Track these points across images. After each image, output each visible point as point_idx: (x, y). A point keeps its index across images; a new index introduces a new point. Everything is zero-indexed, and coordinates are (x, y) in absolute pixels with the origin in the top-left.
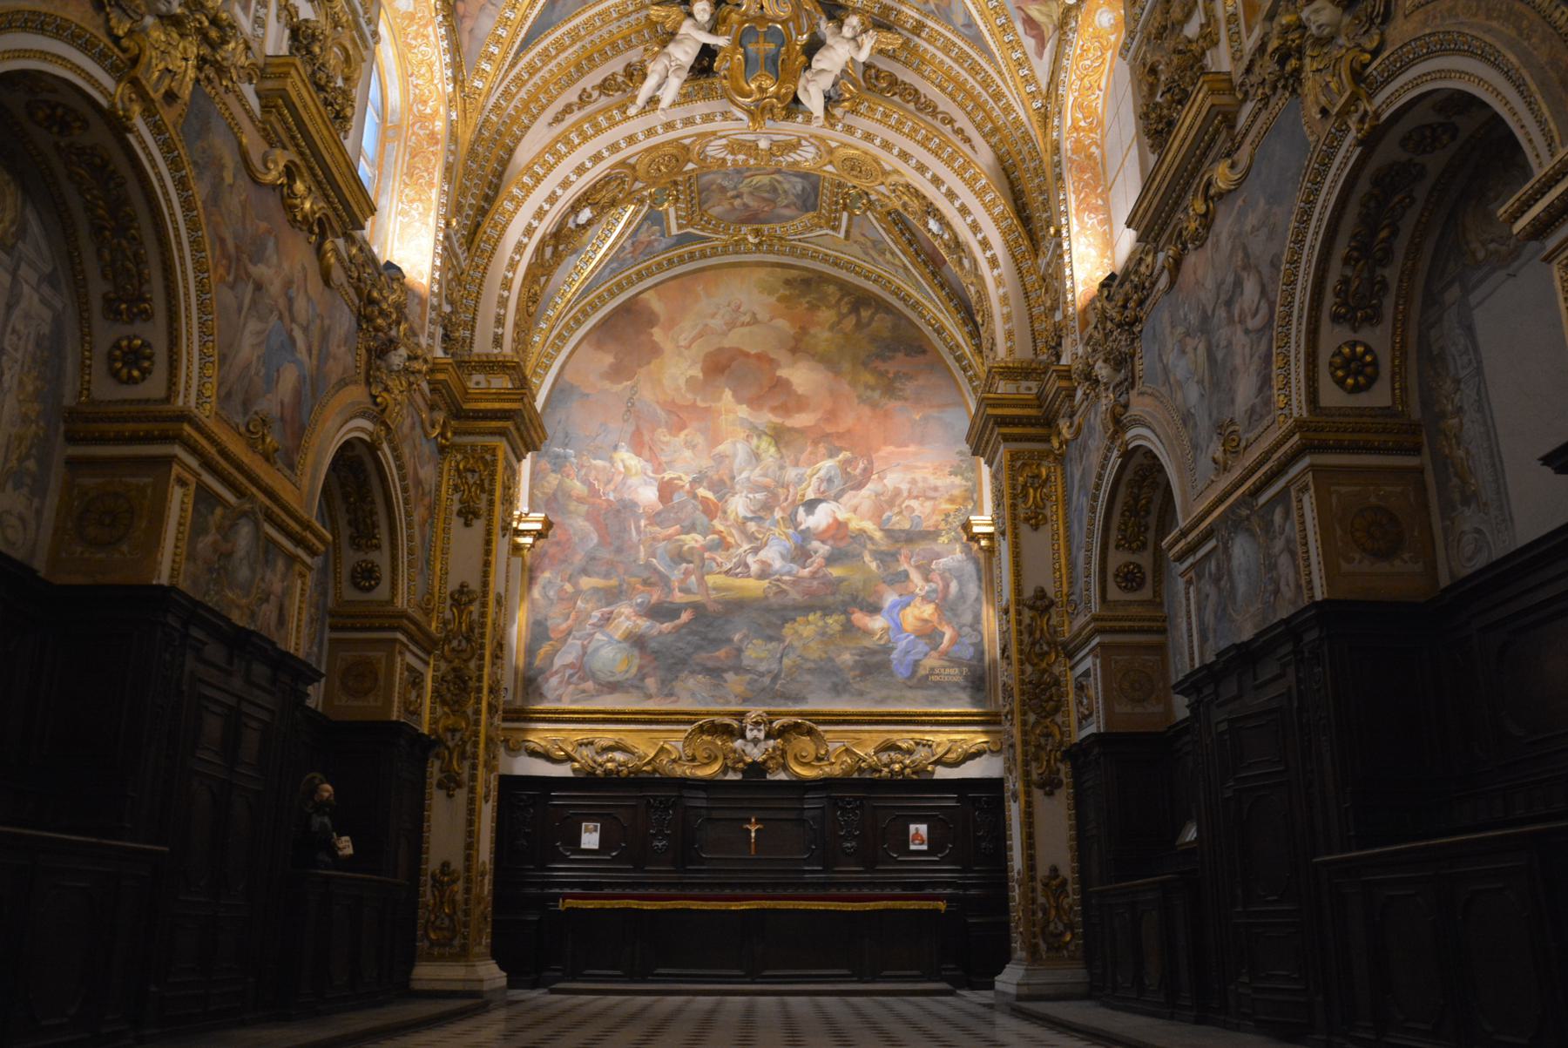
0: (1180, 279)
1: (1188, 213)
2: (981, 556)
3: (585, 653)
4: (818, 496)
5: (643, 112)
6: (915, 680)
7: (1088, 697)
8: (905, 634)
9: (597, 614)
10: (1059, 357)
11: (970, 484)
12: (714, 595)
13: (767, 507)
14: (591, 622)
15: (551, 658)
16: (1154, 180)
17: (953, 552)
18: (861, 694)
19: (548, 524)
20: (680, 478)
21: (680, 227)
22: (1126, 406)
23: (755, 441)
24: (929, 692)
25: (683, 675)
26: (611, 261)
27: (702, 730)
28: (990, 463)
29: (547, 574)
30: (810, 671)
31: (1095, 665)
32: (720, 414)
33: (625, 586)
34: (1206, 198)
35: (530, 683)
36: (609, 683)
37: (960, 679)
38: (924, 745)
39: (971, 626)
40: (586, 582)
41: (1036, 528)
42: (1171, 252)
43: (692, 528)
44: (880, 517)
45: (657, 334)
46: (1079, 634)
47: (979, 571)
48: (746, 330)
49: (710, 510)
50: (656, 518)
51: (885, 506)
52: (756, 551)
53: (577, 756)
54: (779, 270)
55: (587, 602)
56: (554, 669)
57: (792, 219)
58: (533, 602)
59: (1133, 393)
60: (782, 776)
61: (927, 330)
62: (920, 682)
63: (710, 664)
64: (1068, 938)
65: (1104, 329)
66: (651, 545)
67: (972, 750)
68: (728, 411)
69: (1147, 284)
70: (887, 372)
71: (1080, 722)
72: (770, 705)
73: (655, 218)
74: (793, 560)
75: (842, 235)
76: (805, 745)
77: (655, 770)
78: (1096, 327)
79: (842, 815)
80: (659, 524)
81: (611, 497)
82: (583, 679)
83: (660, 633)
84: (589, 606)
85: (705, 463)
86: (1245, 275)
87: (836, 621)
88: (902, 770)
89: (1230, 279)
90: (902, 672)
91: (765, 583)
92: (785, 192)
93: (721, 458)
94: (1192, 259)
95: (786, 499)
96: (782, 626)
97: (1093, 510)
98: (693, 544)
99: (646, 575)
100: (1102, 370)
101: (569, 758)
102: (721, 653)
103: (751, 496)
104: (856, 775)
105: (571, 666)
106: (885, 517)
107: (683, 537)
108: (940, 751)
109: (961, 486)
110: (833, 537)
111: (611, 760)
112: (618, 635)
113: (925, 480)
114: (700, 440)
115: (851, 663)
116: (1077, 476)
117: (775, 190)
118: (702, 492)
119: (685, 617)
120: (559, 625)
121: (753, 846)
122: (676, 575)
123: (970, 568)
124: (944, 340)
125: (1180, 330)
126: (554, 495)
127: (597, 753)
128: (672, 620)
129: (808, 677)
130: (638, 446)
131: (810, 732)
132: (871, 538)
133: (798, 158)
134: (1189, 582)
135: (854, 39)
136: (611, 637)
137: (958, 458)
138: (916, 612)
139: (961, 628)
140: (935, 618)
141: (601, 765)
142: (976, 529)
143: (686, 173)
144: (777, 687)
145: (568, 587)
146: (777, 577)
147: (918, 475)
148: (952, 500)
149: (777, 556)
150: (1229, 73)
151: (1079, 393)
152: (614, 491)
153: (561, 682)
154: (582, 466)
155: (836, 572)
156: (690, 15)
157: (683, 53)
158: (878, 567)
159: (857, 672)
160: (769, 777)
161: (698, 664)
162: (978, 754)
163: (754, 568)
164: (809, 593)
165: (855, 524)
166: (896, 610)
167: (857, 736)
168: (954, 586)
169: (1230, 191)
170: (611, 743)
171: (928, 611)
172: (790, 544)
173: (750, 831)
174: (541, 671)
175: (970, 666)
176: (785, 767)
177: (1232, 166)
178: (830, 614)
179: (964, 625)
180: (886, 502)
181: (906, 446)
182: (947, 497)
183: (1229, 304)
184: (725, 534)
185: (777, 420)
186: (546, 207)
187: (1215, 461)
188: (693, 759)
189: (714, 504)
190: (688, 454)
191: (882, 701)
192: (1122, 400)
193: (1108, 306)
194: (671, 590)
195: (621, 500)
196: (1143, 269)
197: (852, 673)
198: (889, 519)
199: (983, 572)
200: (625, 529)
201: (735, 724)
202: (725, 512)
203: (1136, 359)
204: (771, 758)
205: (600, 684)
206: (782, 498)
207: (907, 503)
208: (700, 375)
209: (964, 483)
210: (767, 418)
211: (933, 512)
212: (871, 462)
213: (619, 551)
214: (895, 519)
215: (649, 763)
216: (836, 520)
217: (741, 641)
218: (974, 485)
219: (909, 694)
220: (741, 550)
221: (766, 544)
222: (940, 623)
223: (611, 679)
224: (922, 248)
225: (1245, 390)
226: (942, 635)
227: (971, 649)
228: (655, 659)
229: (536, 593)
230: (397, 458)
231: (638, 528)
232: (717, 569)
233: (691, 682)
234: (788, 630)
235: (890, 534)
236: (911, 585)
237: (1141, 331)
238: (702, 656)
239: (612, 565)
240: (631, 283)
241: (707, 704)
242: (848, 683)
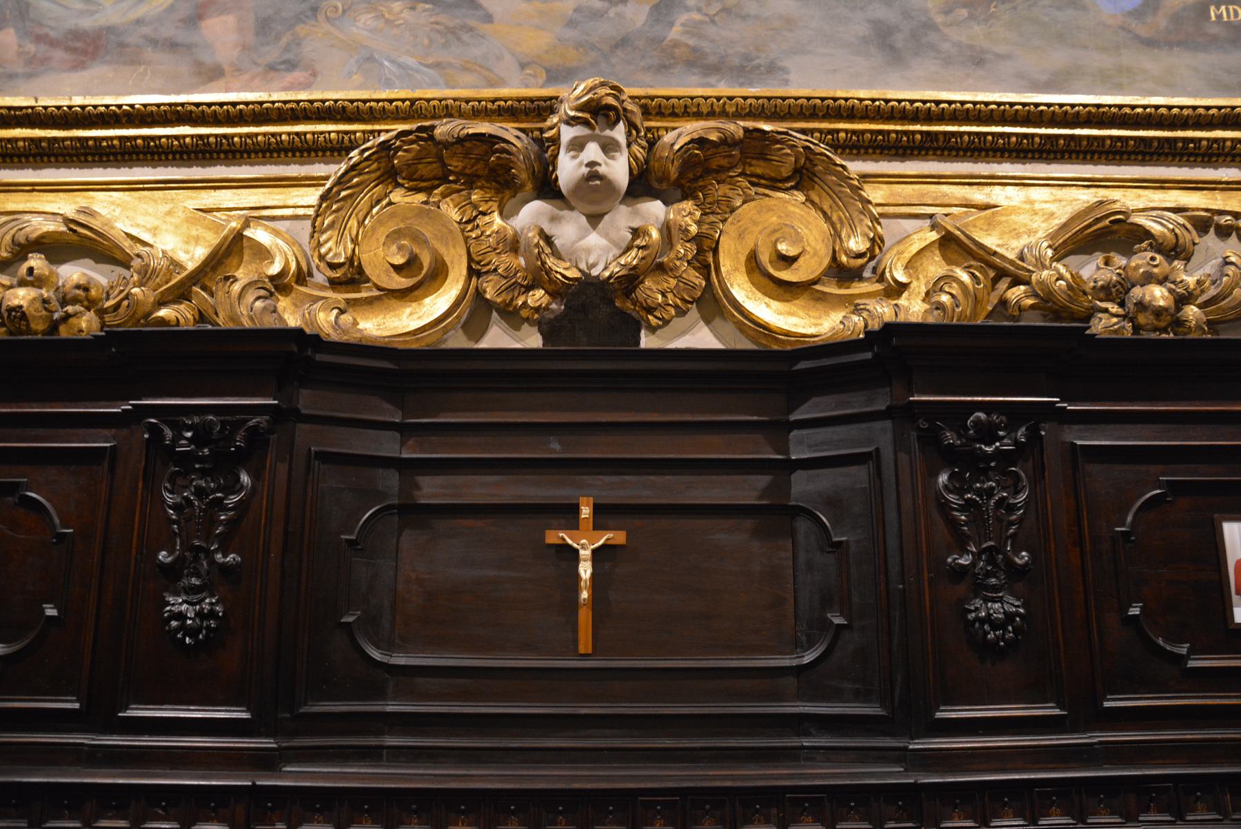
6: (1162, 21)
36: (77, 35)
79: (958, 485)
121: (585, 618)
144: (675, 33)
160: (647, 341)
167: (979, 195)
173: (573, 555)
215: (181, 294)
223: (87, 23)
242: (930, 26)
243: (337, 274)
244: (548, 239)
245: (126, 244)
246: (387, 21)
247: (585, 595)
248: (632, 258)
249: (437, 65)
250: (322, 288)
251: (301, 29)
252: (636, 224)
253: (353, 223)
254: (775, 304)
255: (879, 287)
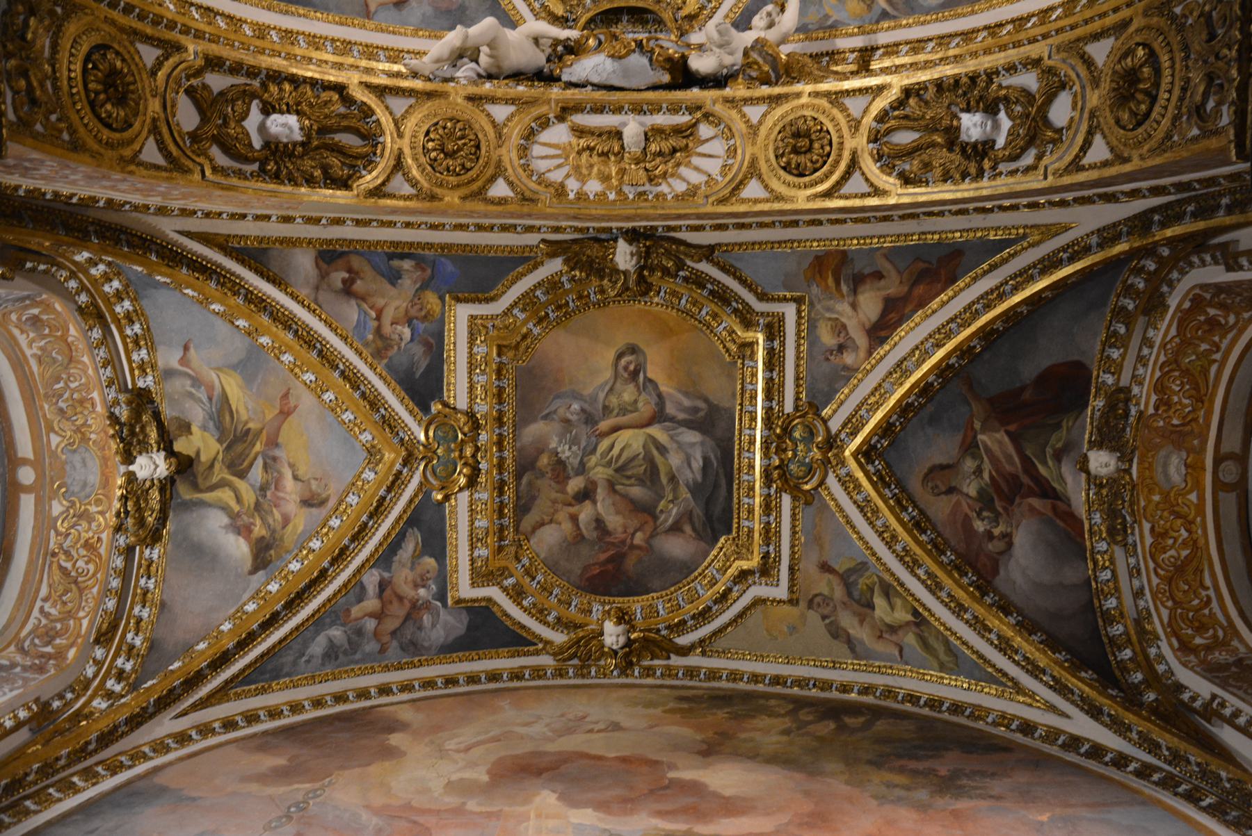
48: (601, 735)
54: (666, 691)
57: (685, 569)
75: (781, 592)
92: (673, 479)
117: (653, 470)
133: (696, 178)
143: (492, 202)
208: (485, 778)
224: (946, 542)
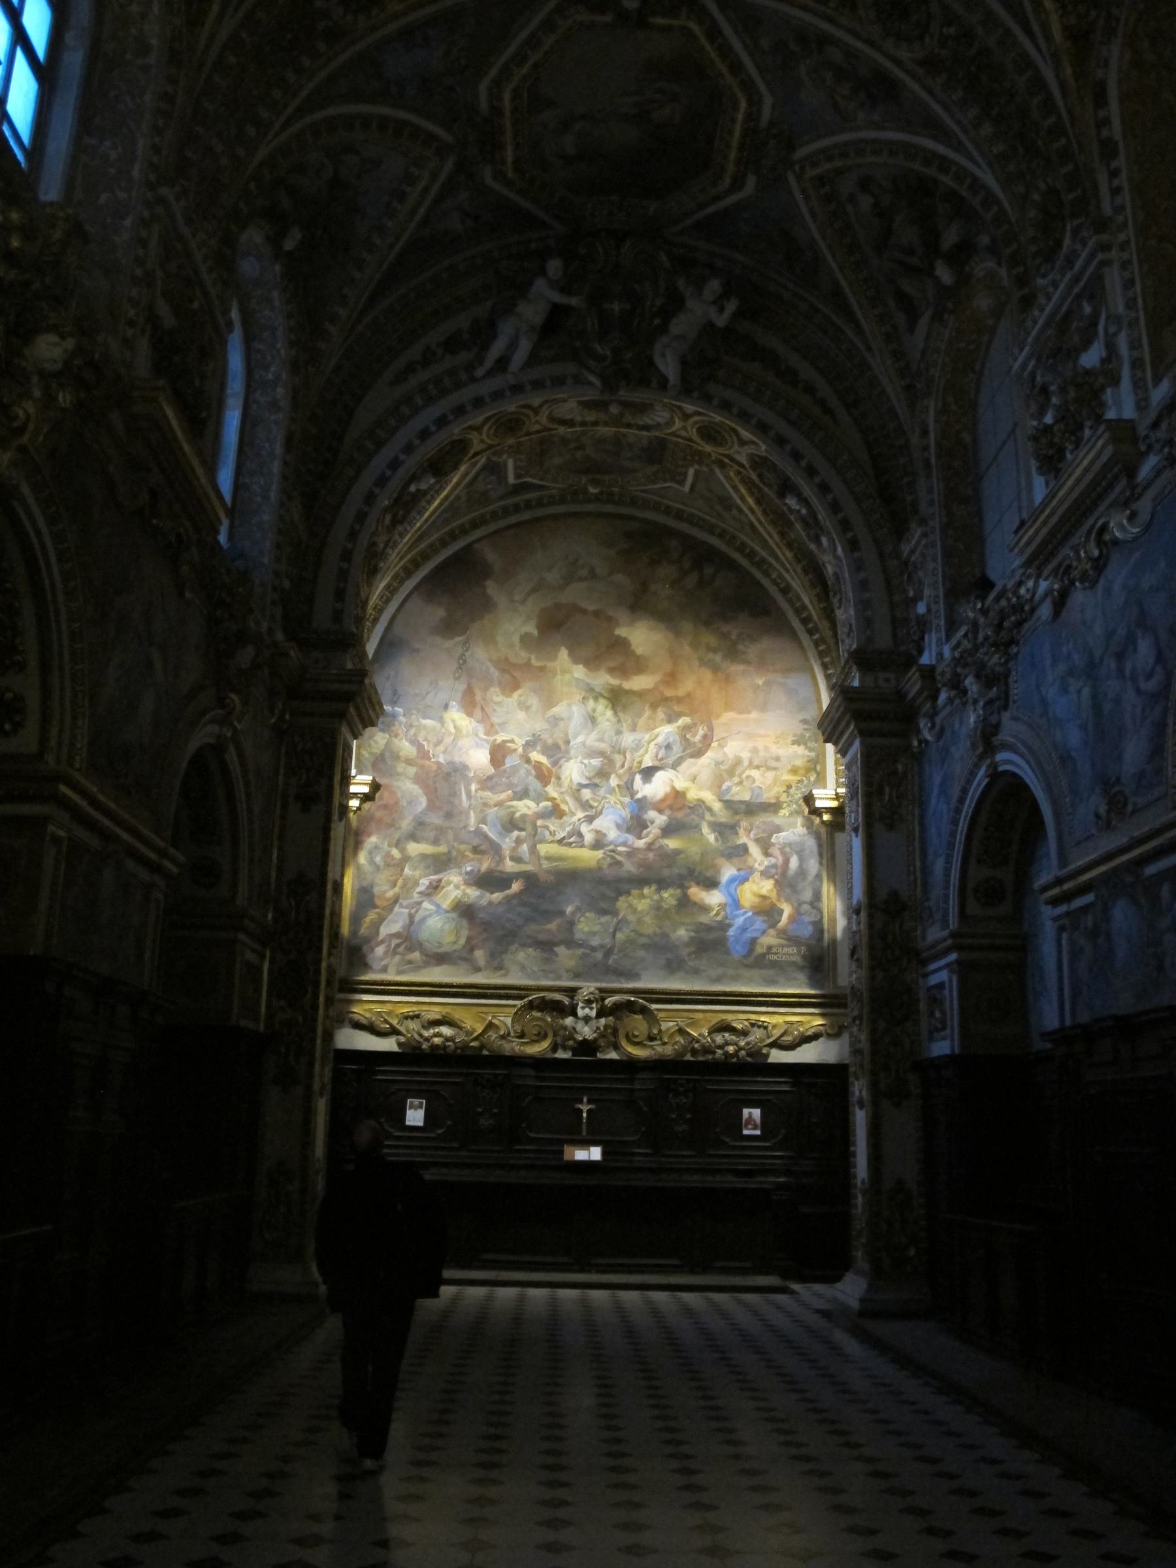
0: (1064, 614)
1: (1077, 553)
2: (823, 830)
3: (411, 922)
4: (656, 763)
5: (489, 373)
6: (751, 959)
7: (943, 1012)
8: (741, 911)
9: (424, 882)
10: (921, 651)
11: (813, 754)
12: (546, 865)
13: (603, 774)
14: (419, 889)
15: (376, 925)
16: (1042, 512)
17: (794, 825)
18: (696, 972)
19: (375, 787)
20: (512, 741)
21: (518, 476)
22: (997, 727)
23: (591, 703)
24: (763, 971)
25: (513, 948)
26: (444, 511)
27: (531, 1006)
28: (843, 752)
29: (373, 839)
30: (645, 947)
31: (951, 981)
32: (555, 674)
33: (454, 853)
34: (1100, 542)
35: (357, 955)
36: (437, 954)
37: (797, 959)
38: (759, 1027)
39: (811, 904)
40: (414, 848)
41: (891, 827)
42: (1056, 586)
43: (523, 794)
44: (720, 787)
45: (491, 587)
46: (933, 946)
47: (820, 846)
49: (543, 776)
50: (487, 783)
51: (725, 775)
52: (590, 819)
53: (402, 1029)
55: (415, 869)
56: (380, 938)
58: (359, 867)
59: (1006, 716)
60: (613, 1055)
61: (774, 591)
62: (758, 961)
63: (542, 937)
64: (912, 1252)
65: (976, 638)
66: (482, 811)
67: (809, 1033)
68: (564, 672)
69: (1027, 608)
70: (729, 633)
71: (931, 1033)
72: (601, 981)
73: (494, 469)
74: (629, 830)
75: (687, 488)
76: (637, 1023)
77: (482, 1047)
78: (966, 635)
80: (491, 789)
81: (441, 759)
82: (410, 949)
83: (490, 903)
84: (417, 873)
85: (539, 725)
86: (1139, 633)
87: (671, 895)
88: (737, 1052)
89: (1122, 632)
90: (738, 951)
91: (599, 854)
93: (556, 721)
94: (1079, 597)
95: (623, 766)
96: (617, 899)
97: (955, 822)
98: (525, 811)
99: (476, 842)
100: (970, 683)
101: (394, 1032)
102: (552, 926)
103: (586, 761)
104: (689, 1057)
105: (397, 935)
106: (724, 787)
107: (514, 803)
108: (776, 1033)
109: (803, 756)
110: (671, 807)
111: (438, 1035)
112: (446, 905)
113: (766, 748)
114: (534, 701)
115: (686, 939)
116: (937, 780)
118: (536, 756)
119: (516, 887)
120: (385, 892)
121: (584, 1127)
122: (507, 844)
123: (811, 843)
124: (790, 602)
125: (1062, 668)
126: (382, 755)
127: (423, 1027)
128: (502, 891)
129: (641, 953)
130: (469, 704)
131: (644, 1011)
132: (710, 810)
134: (1062, 929)
135: (714, 302)
136: (438, 906)
137: (801, 727)
138: (755, 888)
139: (800, 905)
140: (774, 895)
141: (427, 1040)
142: (819, 804)
144: (610, 962)
145: (395, 853)
146: (611, 847)
147: (760, 744)
148: (794, 771)
149: (613, 826)
150: (1131, 421)
151: (943, 696)
152: (445, 752)
153: (386, 953)
154: (411, 726)
155: (672, 844)
156: (543, 272)
157: (532, 312)
158: (717, 840)
159: (693, 949)
160: (599, 1055)
161: (529, 937)
162: (815, 1037)
163: (589, 837)
164: (644, 864)
165: (693, 795)
166: (734, 885)
167: (691, 1015)
168: (794, 862)
169: (1126, 542)
170: (438, 1017)
171: (767, 887)
172: (626, 813)
173: (581, 1111)
174: (367, 940)
175: (809, 947)
176: (616, 1047)
177: (1132, 517)
178: (667, 888)
179: (805, 903)
180: (726, 771)
181: (749, 712)
182: (789, 767)
183: (1120, 656)
184: (558, 801)
185: (615, 682)
186: (389, 473)
187: (1098, 816)
188: (522, 1035)
189: (548, 769)
190: (521, 715)
191: (718, 980)
192: (993, 719)
193: (982, 620)
194: (501, 859)
195: (451, 763)
196: (1022, 591)
197: (687, 950)
198: (729, 788)
199: (825, 850)
200: (454, 794)
201: (566, 1001)
202: (559, 778)
203: (1011, 680)
204: (603, 1035)
205: (427, 955)
206: (618, 764)
207: (747, 773)
208: (535, 632)
209: (807, 752)
210: (603, 679)
211: (775, 781)
212: (711, 729)
213: (449, 815)
214: (735, 789)
215: (476, 1039)
216: (673, 788)
217: (573, 913)
218: (817, 756)
219: (746, 973)
220: (575, 819)
221: (601, 813)
222: (779, 900)
225: (1134, 752)
226: (781, 912)
227: (810, 928)
228: (485, 930)
229: (362, 858)
230: (241, 755)
231: (469, 796)
232: (550, 838)
233: (521, 956)
234: (622, 903)
235: (729, 804)
236: (750, 861)
237: (1016, 654)
238: (531, 929)
239: (441, 831)
240: (464, 531)
241: (538, 979)
243: (518, 1035)
244: (574, 1029)
245: (459, 1022)
246: (528, 955)
247: (584, 1121)
248: (595, 1035)
249: (543, 970)
250: (513, 1037)
251: (503, 956)
252: (598, 1025)
253: (522, 1020)
254: (633, 1047)
255: (660, 1042)
